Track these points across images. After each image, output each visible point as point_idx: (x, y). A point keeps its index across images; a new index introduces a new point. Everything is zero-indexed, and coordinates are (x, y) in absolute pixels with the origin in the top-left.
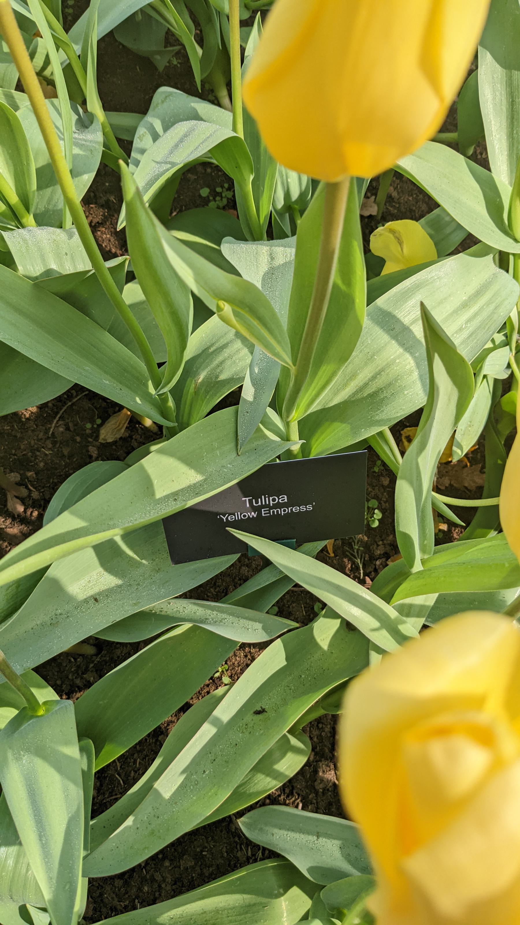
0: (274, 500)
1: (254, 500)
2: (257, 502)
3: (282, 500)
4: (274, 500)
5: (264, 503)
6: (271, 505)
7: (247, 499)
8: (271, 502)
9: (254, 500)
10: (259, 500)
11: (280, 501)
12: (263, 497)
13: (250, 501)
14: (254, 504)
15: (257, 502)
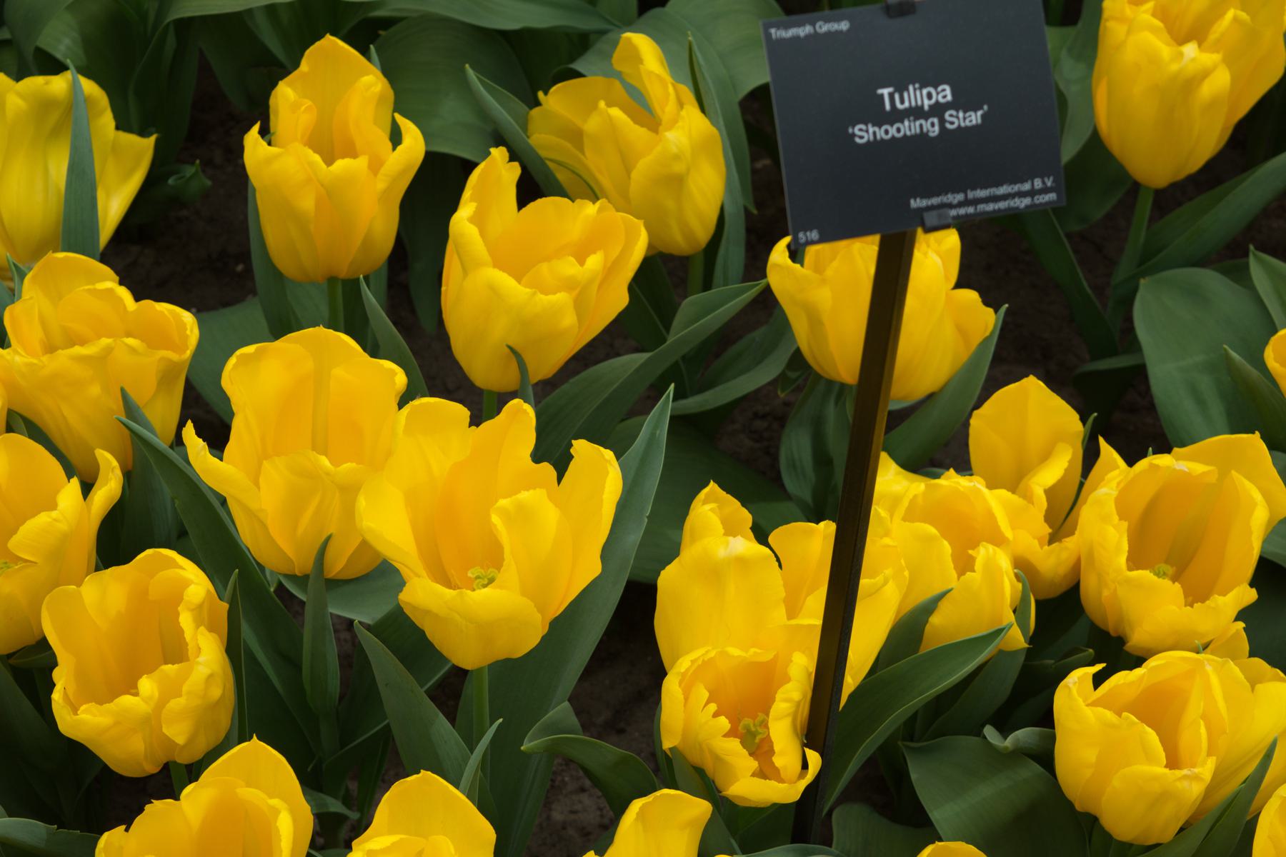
0: (930, 96)
1: (897, 96)
2: (902, 102)
3: (945, 97)
4: (930, 96)
5: (913, 104)
6: (926, 108)
7: (885, 92)
8: (926, 103)
9: (897, 96)
10: (906, 95)
11: (941, 100)
12: (911, 88)
13: (891, 96)
14: (899, 106)
15: (902, 102)
